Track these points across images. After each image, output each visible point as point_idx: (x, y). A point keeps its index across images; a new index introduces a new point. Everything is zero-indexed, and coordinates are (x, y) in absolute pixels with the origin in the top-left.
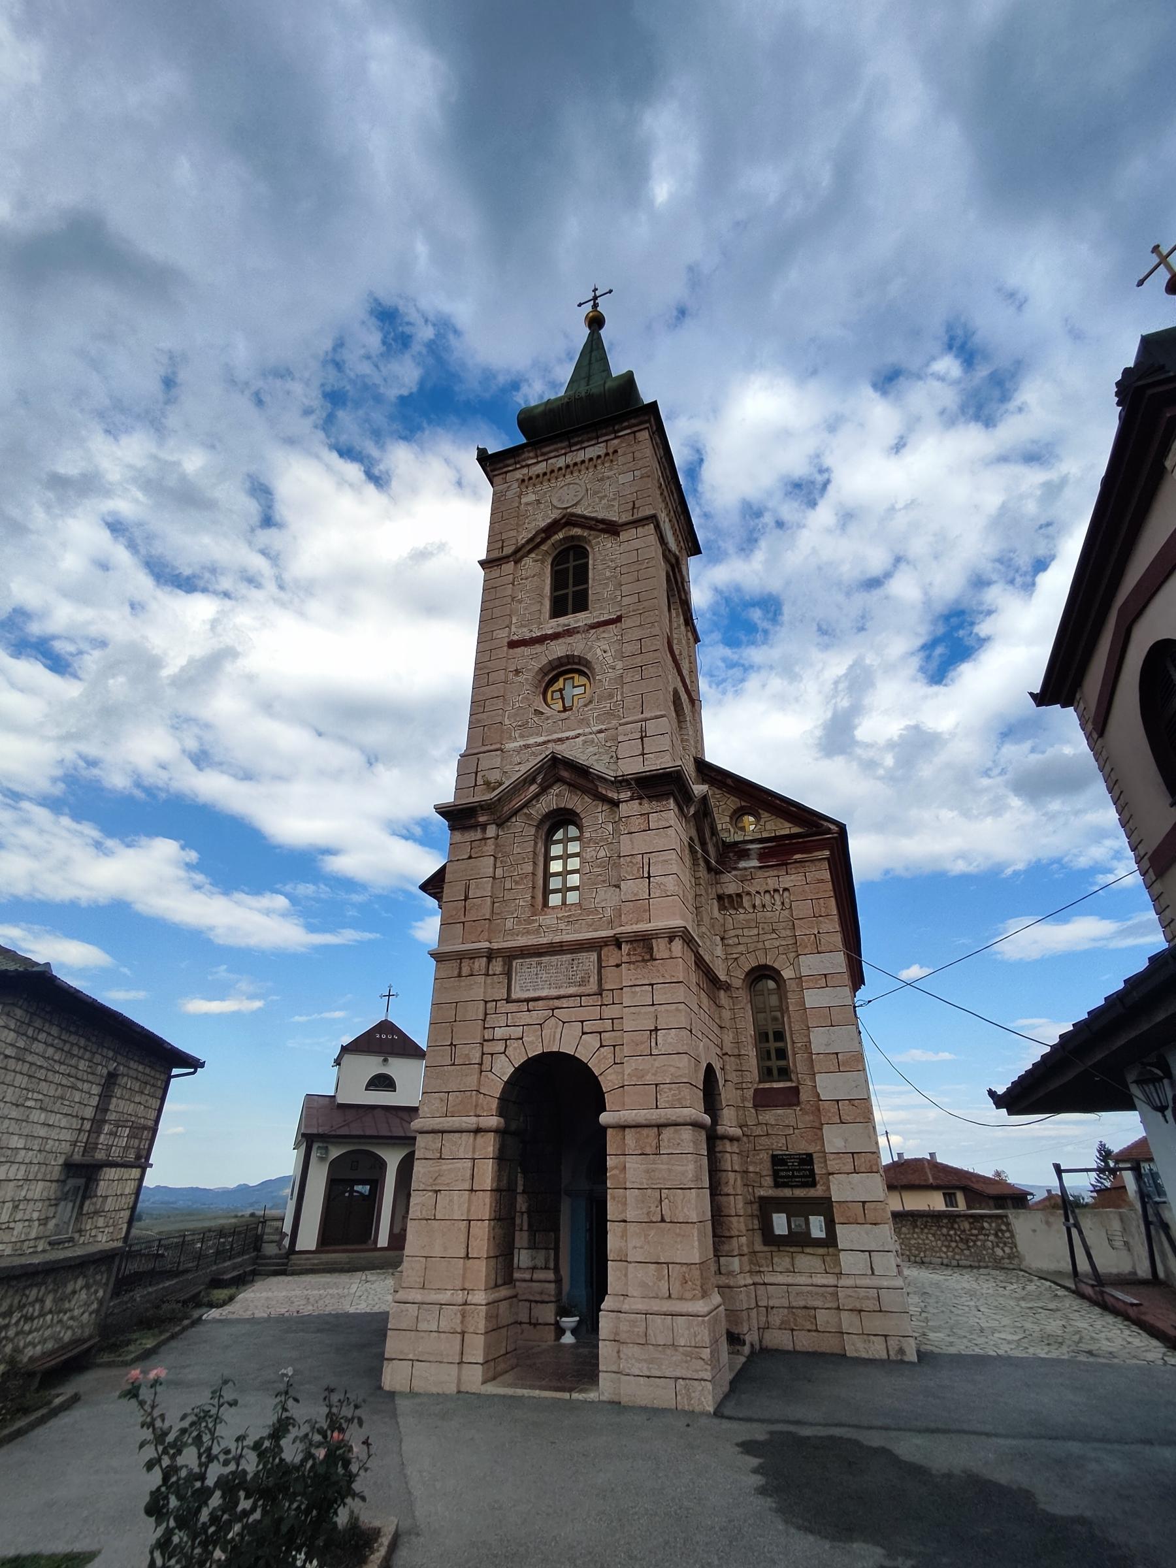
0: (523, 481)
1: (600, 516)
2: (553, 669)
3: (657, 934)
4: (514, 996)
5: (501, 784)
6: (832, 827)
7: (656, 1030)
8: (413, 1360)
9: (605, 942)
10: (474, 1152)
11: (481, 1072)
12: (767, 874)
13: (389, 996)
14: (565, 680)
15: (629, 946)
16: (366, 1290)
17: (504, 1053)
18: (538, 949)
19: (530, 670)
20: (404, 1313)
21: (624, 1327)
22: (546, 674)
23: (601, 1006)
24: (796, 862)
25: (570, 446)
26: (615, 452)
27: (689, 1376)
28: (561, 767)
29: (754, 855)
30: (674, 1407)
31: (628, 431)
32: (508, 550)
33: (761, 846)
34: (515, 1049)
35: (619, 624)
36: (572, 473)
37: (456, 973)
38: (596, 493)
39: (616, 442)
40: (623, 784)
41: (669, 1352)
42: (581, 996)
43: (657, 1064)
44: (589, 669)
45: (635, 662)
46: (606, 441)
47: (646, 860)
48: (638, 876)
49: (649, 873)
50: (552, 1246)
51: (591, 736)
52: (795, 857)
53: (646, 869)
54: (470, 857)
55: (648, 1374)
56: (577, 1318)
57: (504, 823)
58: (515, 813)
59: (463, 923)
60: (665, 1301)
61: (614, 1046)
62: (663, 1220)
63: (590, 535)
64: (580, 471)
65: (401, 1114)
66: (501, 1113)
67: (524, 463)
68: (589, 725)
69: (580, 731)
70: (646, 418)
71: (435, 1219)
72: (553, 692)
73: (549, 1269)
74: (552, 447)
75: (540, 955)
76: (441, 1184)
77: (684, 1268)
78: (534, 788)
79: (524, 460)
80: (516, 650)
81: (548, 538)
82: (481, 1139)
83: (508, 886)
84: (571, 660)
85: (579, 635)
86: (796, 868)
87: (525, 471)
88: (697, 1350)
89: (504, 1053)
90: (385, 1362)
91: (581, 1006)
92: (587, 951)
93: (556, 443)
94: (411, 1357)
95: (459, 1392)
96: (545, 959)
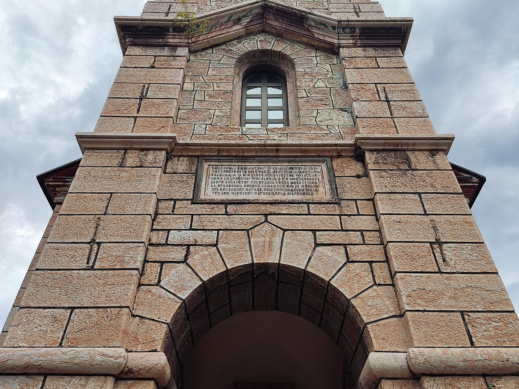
3: (414, 144)
4: (202, 197)
11: (140, 285)
17: (185, 261)
18: (243, 151)
23: (340, 215)
40: (347, 30)
43: (453, 284)
49: (386, 97)
54: (152, 67)
59: (135, 118)
61: (371, 263)
75: (244, 159)
89: (185, 261)
91: (309, 214)
96: (251, 166)
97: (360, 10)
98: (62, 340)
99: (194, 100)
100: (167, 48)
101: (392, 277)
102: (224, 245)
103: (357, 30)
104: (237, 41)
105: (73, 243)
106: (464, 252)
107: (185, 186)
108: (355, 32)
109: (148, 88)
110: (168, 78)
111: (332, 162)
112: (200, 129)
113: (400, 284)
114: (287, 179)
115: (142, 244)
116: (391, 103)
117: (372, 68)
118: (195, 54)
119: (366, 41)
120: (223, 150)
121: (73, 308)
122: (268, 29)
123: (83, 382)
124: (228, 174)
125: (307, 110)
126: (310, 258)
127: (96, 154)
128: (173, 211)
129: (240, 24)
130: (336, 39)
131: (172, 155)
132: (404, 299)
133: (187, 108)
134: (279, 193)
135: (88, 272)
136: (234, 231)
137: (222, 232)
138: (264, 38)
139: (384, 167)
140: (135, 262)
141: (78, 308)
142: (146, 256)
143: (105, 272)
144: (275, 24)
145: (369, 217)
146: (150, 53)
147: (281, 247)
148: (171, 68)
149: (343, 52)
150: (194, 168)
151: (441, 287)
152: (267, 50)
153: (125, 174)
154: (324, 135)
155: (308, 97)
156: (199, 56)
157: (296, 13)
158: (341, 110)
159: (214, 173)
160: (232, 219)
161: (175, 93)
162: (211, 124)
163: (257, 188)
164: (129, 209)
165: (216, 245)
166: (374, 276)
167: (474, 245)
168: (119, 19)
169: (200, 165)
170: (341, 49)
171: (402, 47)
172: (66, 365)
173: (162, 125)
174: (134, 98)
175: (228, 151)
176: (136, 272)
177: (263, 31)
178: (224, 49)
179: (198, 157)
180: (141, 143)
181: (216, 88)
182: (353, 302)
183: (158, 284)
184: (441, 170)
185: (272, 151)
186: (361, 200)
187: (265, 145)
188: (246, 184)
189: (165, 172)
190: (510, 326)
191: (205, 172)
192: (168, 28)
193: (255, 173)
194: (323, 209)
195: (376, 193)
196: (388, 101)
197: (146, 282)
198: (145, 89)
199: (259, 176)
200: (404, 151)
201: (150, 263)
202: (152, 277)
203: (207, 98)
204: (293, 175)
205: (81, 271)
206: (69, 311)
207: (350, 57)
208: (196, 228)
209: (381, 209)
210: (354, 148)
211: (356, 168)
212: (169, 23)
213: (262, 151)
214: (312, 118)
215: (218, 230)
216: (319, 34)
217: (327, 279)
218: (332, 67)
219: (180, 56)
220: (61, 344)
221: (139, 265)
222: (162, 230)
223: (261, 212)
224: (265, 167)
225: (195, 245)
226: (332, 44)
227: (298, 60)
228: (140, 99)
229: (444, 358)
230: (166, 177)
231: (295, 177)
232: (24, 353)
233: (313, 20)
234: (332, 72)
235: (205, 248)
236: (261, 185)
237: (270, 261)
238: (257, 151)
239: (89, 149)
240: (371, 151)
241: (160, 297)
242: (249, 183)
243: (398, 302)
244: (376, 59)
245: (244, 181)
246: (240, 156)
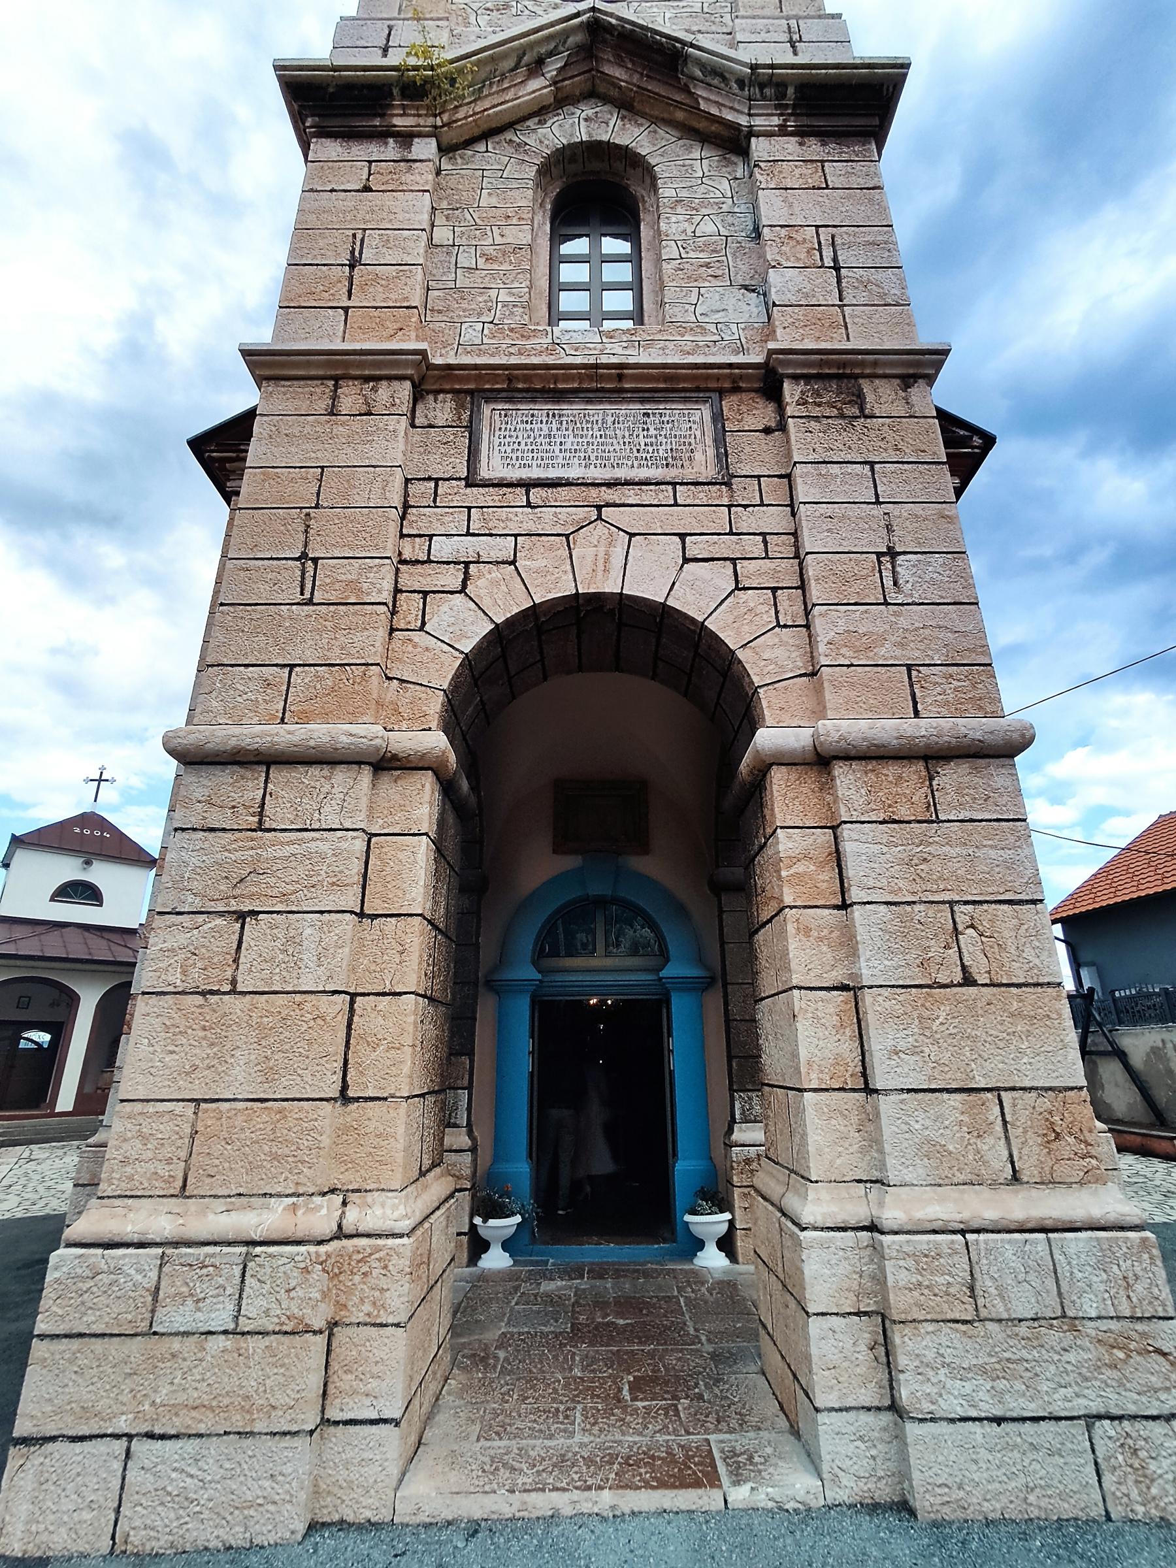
3: (875, 364)
4: (484, 473)
7: (892, 553)
8: (130, 1437)
9: (734, 379)
10: (370, 817)
11: (392, 630)
13: (100, 780)
15: (799, 388)
16: (26, 1174)
17: (463, 591)
18: (556, 379)
20: (105, 1278)
21: (898, 1275)
23: (729, 506)
27: (1132, 1409)
30: (1097, 1512)
34: (495, 583)
37: (322, 405)
40: (767, 91)
41: (1053, 1337)
42: (674, 484)
43: (903, 622)
47: (825, 234)
49: (835, 260)
50: (466, 1083)
53: (828, 253)
54: (367, 189)
55: (998, 1412)
56: (518, 1219)
59: (346, 309)
60: (1006, 1194)
61: (774, 590)
62: (968, 980)
65: (106, 935)
66: (452, 723)
71: (233, 992)
73: (456, 1126)
75: (558, 396)
76: (251, 896)
77: (1045, 1103)
78: (537, 87)
82: (392, 789)
83: (465, 260)
88: (1140, 1327)
89: (463, 591)
90: (12, 1451)
91: (676, 504)
92: (686, 400)
94: (122, 1424)
95: (314, 1527)
96: (571, 410)
97: (800, 37)
98: (284, 714)
99: (457, 268)
100: (391, 140)
101: (807, 613)
102: (528, 563)
103: (791, 91)
104: (536, 119)
105: (271, 559)
106: (930, 569)
107: (452, 452)
108: (783, 96)
109: (362, 241)
110: (400, 216)
111: (721, 401)
112: (471, 334)
113: (819, 625)
114: (638, 436)
115: (388, 561)
117: (814, 188)
118: (451, 155)
119: (805, 121)
120: (517, 378)
121: (292, 666)
122: (602, 88)
123: (326, 772)
124: (529, 427)
126: (674, 583)
127: (283, 389)
128: (435, 501)
129: (543, 75)
130: (742, 113)
131: (422, 390)
132: (822, 648)
134: (623, 464)
135: (306, 608)
136: (543, 538)
137: (523, 538)
138: (594, 111)
139: (816, 411)
140: (380, 592)
141: (300, 665)
142: (396, 582)
143: (332, 608)
144: (617, 72)
145: (780, 508)
146: (358, 153)
147: (626, 564)
148: (404, 191)
149: (759, 148)
150: (466, 416)
151: (881, 628)
152: (600, 142)
153: (341, 429)
154: (710, 344)
155: (682, 258)
156: (459, 161)
157: (662, 44)
159: (503, 426)
160: (539, 515)
161: (417, 251)
162: (491, 322)
163: (582, 455)
164: (357, 497)
165: (513, 563)
166: (777, 612)
167: (949, 556)
168: (284, 68)
169: (475, 409)
170: (753, 140)
171: (878, 134)
172: (296, 749)
173: (399, 325)
174: (338, 265)
175: (526, 379)
176: (383, 608)
177: (591, 94)
178: (510, 140)
179: (471, 392)
180: (361, 365)
181: (498, 240)
182: (740, 654)
183: (421, 629)
184: (916, 417)
185: (609, 378)
186: (768, 476)
187: (596, 366)
188: (563, 447)
189: (413, 426)
190: (980, 686)
191: (486, 422)
192: (391, 90)
193: (578, 425)
194: (702, 495)
195: (795, 463)
196: (837, 268)
197: (402, 626)
198: (358, 243)
199: (585, 432)
200: (856, 377)
201: (404, 594)
202: (411, 618)
203: (481, 261)
204: (648, 429)
205: (294, 607)
206: (287, 670)
208: (477, 532)
209: (803, 492)
210: (763, 371)
211: (763, 414)
212: (392, 75)
213: (590, 378)
214: (687, 306)
215: (516, 536)
216: (710, 102)
217: (700, 619)
218: (734, 185)
219: (420, 161)
220: (283, 719)
221: (386, 596)
222: (420, 536)
223: (591, 501)
224: (596, 412)
225: (478, 562)
226: (735, 127)
227: (664, 168)
228: (350, 266)
229: (870, 734)
230: (417, 435)
231: (652, 432)
232: (230, 732)
234: (732, 197)
235: (495, 568)
236: (590, 450)
237: (607, 590)
238: (581, 378)
239: (269, 379)
240: (796, 378)
241: (427, 649)
242: (568, 446)
243: (812, 653)
244: (823, 167)
245: (558, 441)
246: (550, 390)
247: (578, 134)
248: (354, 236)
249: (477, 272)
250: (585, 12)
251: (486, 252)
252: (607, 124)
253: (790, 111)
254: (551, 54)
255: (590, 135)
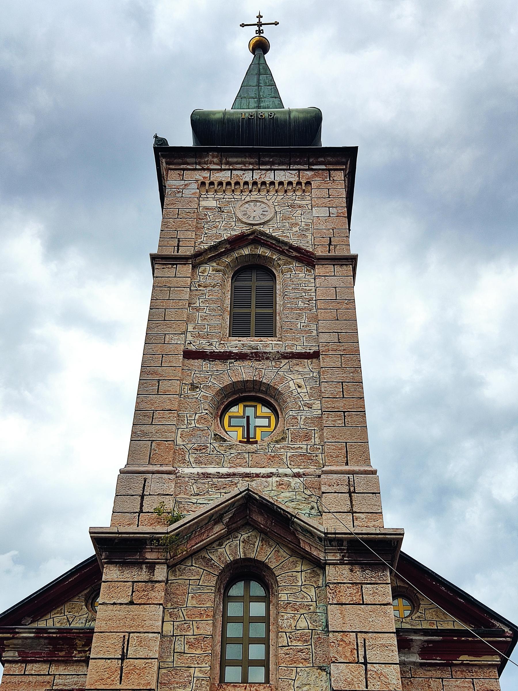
0: (203, 184)
1: (295, 243)
2: (234, 393)
5: (177, 520)
6: (506, 629)
12: (429, 674)
14: (245, 406)
19: (209, 387)
22: (227, 396)
24: (462, 664)
25: (259, 164)
26: (308, 183)
28: (255, 508)
29: (416, 648)
31: (324, 167)
32: (186, 251)
33: (426, 638)
35: (314, 360)
36: (259, 191)
38: (285, 218)
39: (310, 173)
44: (276, 400)
45: (336, 405)
46: (299, 170)
47: (360, 641)
48: (351, 660)
49: (365, 657)
51: (286, 479)
52: (462, 658)
53: (361, 652)
54: (131, 603)
57: (175, 565)
58: (192, 555)
63: (279, 259)
64: (268, 191)
67: (206, 167)
68: (281, 463)
69: (274, 470)
70: (344, 160)
72: (230, 417)
74: (240, 160)
78: (219, 529)
79: (205, 163)
80: (192, 361)
81: (232, 250)
84: (256, 387)
85: (268, 361)
86: (462, 672)
87: (206, 174)
93: (245, 157)
97: (354, 489)
99: (174, 652)
100: (144, 566)
103: (345, 543)
104: (217, 543)
116: (369, 665)
118: (173, 569)
125: (286, 669)
133: (167, 666)
138: (247, 535)
148: (150, 604)
158: (321, 669)
170: (327, 567)
178: (204, 557)
198: (126, 643)
207: (335, 583)
214: (290, 681)
218: (317, 591)
233: (299, 525)
234: (316, 602)
247: (239, 553)
248: (124, 636)
249: (185, 655)
250: (244, 491)
251: (190, 640)
252: (254, 545)
253: (346, 551)
254: (227, 512)
255: (245, 555)
